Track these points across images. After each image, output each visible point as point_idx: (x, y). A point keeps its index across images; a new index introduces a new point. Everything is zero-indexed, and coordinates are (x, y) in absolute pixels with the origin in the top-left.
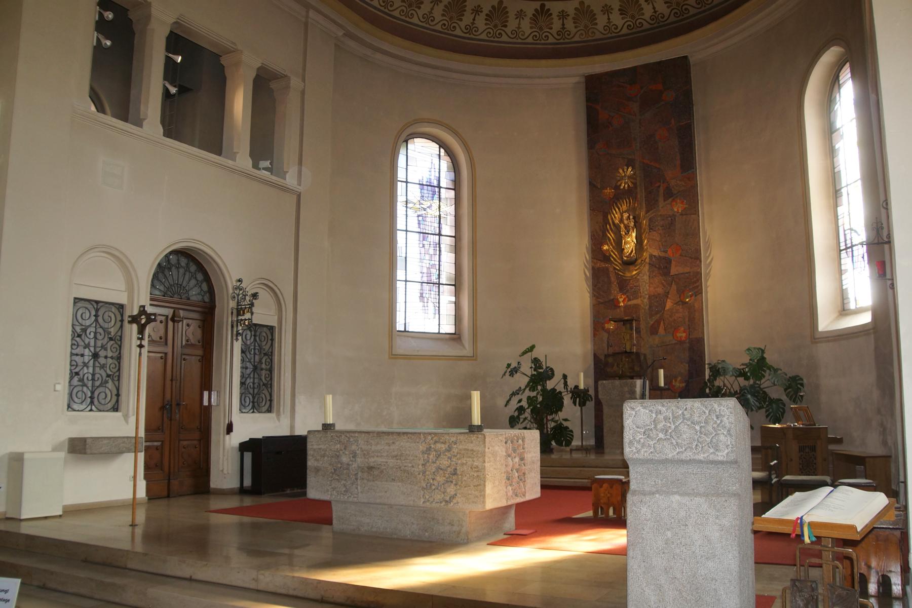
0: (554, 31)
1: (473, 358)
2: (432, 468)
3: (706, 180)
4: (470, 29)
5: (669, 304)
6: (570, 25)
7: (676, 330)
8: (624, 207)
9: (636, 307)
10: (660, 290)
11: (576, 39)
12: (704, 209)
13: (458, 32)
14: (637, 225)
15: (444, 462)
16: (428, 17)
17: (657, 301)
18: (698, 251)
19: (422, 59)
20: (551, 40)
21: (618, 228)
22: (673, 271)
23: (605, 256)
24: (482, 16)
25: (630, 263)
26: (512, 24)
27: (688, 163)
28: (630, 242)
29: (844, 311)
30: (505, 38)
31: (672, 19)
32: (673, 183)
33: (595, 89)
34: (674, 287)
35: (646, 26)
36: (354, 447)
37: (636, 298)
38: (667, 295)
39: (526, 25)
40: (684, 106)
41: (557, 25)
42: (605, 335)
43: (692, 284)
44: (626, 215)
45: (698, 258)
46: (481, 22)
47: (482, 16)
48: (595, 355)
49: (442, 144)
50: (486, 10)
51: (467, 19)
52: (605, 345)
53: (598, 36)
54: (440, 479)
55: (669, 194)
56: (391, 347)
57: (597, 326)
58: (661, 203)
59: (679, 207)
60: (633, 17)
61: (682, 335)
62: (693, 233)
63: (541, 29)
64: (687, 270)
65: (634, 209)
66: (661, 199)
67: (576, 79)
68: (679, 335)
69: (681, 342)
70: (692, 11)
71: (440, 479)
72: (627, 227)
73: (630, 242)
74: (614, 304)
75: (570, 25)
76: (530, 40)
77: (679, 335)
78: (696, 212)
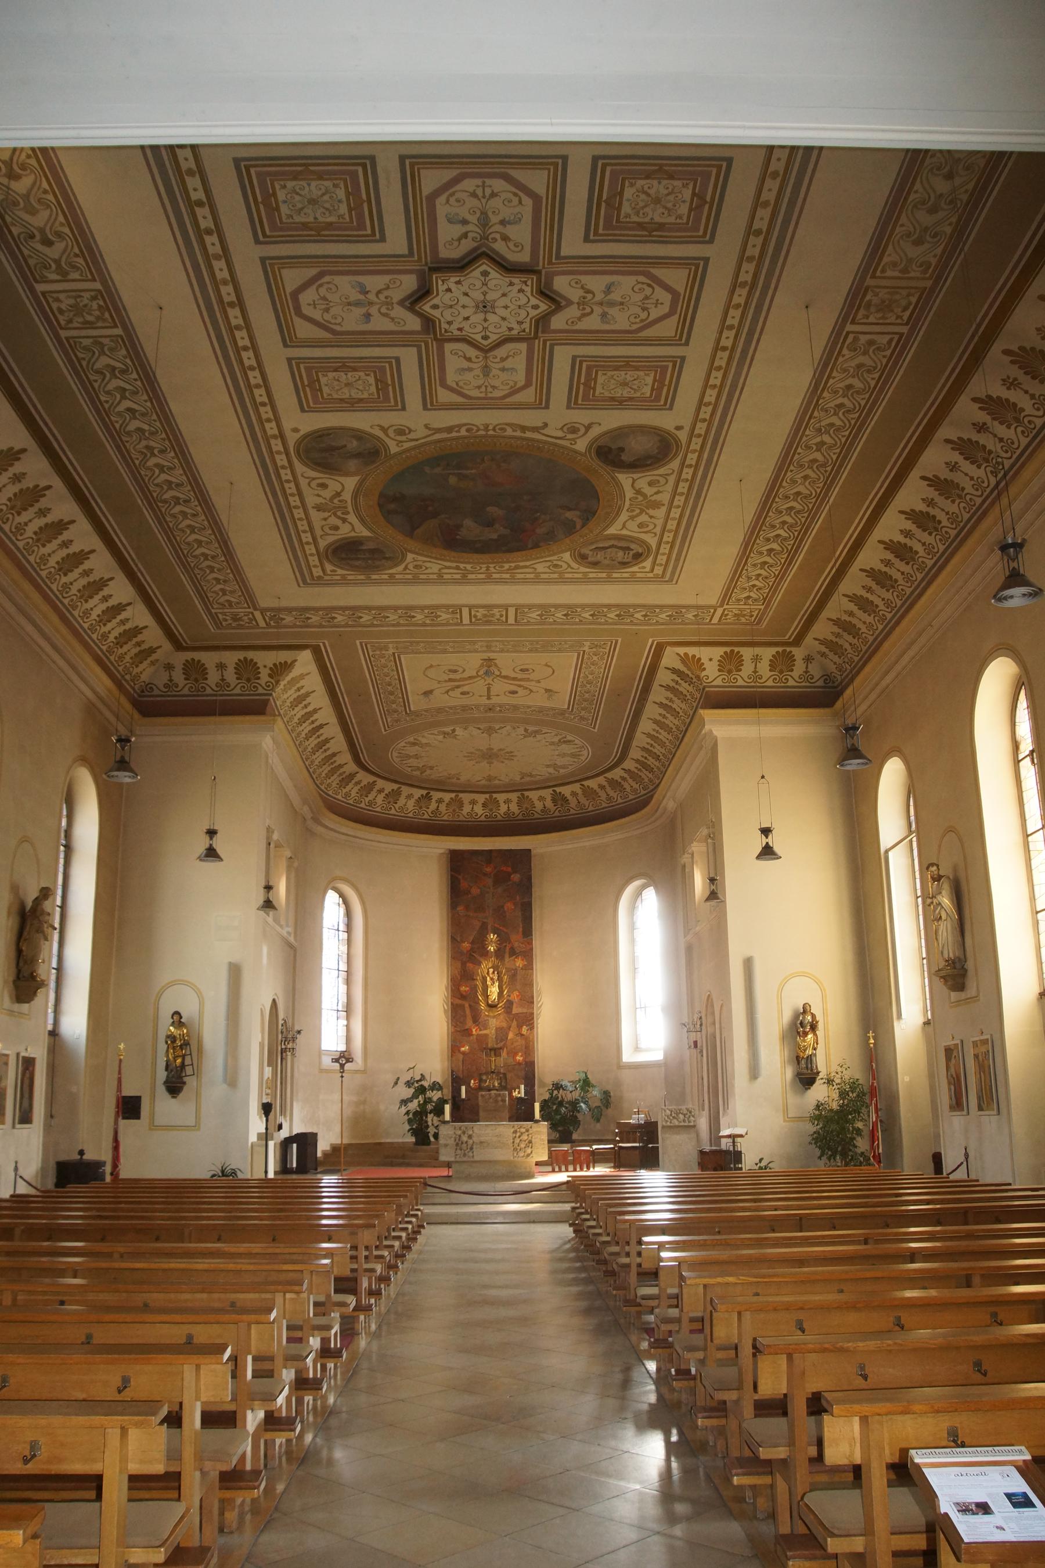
0: (429, 811)
1: (364, 1072)
2: (517, 1141)
3: (539, 944)
4: (370, 803)
5: (511, 1035)
6: (443, 808)
7: (516, 1054)
8: (490, 965)
9: (486, 1035)
10: (504, 1025)
11: (445, 818)
12: (538, 965)
13: (362, 805)
14: (500, 979)
15: (525, 1137)
16: (347, 795)
17: (502, 1034)
18: (533, 997)
19: (343, 830)
20: (426, 816)
21: (484, 979)
22: (515, 1010)
23: (462, 995)
24: (383, 795)
25: (492, 1006)
26: (402, 801)
27: (528, 932)
28: (494, 991)
29: (637, 1049)
30: (393, 812)
31: (520, 817)
32: (516, 944)
33: (456, 861)
34: (515, 1023)
35: (499, 818)
36: (471, 1132)
37: (486, 1029)
38: (509, 1028)
39: (411, 804)
40: (526, 887)
41: (433, 805)
42: (461, 1057)
43: (528, 1020)
44: (491, 970)
45: (533, 1003)
46: (380, 799)
47: (383, 795)
48: (452, 1071)
49: (341, 895)
50: (386, 792)
51: (371, 797)
52: (460, 1064)
53: (461, 818)
54: (523, 1145)
55: (513, 953)
56: (320, 1063)
57: (454, 1049)
58: (507, 959)
59: (519, 963)
60: (491, 810)
61: (519, 1058)
62: (528, 984)
63: (421, 808)
64: (525, 1011)
65: (498, 967)
66: (507, 955)
67: (442, 851)
68: (518, 1058)
69: (519, 1064)
70: (536, 816)
71: (523, 1145)
72: (492, 979)
73: (494, 991)
74: (468, 1032)
75: (443, 808)
76: (410, 815)
77: (518, 1058)
78: (532, 969)
